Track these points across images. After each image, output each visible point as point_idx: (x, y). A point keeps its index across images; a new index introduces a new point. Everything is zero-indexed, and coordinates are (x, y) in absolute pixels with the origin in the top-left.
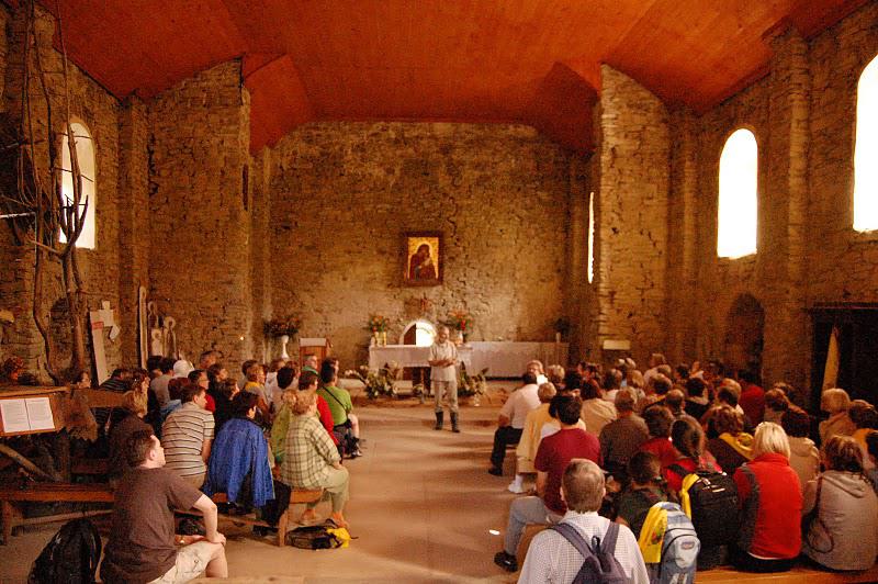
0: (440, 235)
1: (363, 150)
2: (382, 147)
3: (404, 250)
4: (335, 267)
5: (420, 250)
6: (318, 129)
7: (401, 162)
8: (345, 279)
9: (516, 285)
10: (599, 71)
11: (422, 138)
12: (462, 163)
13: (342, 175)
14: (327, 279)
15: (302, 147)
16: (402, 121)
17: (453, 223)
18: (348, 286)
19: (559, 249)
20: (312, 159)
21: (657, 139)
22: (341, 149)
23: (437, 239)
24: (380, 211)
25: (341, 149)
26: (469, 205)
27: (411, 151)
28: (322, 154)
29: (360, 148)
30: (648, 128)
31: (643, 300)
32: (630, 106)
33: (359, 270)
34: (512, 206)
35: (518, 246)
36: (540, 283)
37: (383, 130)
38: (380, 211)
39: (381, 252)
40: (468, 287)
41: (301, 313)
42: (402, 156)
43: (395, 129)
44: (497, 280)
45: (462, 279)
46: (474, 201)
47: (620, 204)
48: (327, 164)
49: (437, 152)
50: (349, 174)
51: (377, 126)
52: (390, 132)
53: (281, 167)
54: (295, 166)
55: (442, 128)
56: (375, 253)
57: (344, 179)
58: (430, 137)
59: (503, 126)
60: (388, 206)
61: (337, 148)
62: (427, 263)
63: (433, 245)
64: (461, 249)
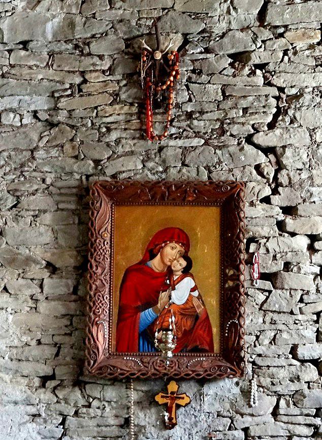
17: (267, 151)
64: (302, 242)
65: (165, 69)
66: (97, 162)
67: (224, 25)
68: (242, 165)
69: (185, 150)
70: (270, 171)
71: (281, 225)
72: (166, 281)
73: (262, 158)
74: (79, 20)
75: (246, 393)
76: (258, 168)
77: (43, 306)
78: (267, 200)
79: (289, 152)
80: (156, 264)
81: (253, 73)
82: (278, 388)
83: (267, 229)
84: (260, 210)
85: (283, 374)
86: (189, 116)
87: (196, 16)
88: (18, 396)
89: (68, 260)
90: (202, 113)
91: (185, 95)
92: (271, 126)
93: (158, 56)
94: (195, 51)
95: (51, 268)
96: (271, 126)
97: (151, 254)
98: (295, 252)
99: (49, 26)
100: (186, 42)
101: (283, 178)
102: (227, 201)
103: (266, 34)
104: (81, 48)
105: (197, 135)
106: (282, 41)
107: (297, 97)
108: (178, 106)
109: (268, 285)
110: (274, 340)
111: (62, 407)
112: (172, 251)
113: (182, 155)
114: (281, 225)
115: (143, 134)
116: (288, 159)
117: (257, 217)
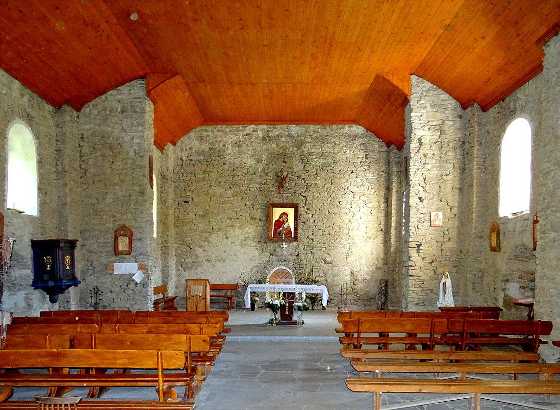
0: (296, 207)
2: (253, 144)
3: (269, 216)
4: (220, 230)
5: (280, 217)
6: (206, 131)
8: (227, 238)
9: (349, 241)
10: (409, 80)
11: (282, 137)
12: (310, 154)
13: (224, 164)
15: (196, 145)
16: (268, 125)
17: (304, 197)
19: (382, 216)
20: (202, 153)
21: (452, 131)
22: (224, 145)
23: (293, 209)
24: (252, 189)
25: (224, 145)
26: (315, 184)
27: (274, 145)
29: (238, 145)
30: (446, 122)
31: (442, 250)
32: (433, 107)
33: (238, 231)
34: (348, 185)
36: (368, 239)
39: (252, 218)
40: (315, 243)
41: (196, 262)
42: (267, 150)
43: (263, 130)
44: (336, 237)
46: (320, 181)
47: (425, 179)
48: (214, 156)
49: (293, 146)
51: (250, 128)
52: (259, 132)
53: (181, 159)
54: (190, 158)
55: (295, 129)
56: (249, 219)
57: (226, 167)
58: (286, 136)
60: (258, 186)
61: (221, 145)
63: (291, 212)
65: (285, 178)
66: (270, 199)
68: (299, 200)
69: (288, 196)
71: (306, 212)
72: (283, 222)
73: (303, 198)
75: (298, 245)
77: (259, 228)
78: (304, 207)
79: (308, 197)
80: (281, 220)
82: (305, 244)
85: (305, 241)
88: (254, 245)
89: (264, 218)
91: (288, 185)
92: (305, 191)
93: (282, 177)
94: (290, 175)
95: (260, 220)
96: (305, 191)
99: (260, 169)
100: (288, 173)
101: (307, 203)
107: (311, 185)
108: (286, 187)
109: (303, 224)
112: (284, 217)
114: (306, 212)
115: (279, 193)
116: (308, 198)
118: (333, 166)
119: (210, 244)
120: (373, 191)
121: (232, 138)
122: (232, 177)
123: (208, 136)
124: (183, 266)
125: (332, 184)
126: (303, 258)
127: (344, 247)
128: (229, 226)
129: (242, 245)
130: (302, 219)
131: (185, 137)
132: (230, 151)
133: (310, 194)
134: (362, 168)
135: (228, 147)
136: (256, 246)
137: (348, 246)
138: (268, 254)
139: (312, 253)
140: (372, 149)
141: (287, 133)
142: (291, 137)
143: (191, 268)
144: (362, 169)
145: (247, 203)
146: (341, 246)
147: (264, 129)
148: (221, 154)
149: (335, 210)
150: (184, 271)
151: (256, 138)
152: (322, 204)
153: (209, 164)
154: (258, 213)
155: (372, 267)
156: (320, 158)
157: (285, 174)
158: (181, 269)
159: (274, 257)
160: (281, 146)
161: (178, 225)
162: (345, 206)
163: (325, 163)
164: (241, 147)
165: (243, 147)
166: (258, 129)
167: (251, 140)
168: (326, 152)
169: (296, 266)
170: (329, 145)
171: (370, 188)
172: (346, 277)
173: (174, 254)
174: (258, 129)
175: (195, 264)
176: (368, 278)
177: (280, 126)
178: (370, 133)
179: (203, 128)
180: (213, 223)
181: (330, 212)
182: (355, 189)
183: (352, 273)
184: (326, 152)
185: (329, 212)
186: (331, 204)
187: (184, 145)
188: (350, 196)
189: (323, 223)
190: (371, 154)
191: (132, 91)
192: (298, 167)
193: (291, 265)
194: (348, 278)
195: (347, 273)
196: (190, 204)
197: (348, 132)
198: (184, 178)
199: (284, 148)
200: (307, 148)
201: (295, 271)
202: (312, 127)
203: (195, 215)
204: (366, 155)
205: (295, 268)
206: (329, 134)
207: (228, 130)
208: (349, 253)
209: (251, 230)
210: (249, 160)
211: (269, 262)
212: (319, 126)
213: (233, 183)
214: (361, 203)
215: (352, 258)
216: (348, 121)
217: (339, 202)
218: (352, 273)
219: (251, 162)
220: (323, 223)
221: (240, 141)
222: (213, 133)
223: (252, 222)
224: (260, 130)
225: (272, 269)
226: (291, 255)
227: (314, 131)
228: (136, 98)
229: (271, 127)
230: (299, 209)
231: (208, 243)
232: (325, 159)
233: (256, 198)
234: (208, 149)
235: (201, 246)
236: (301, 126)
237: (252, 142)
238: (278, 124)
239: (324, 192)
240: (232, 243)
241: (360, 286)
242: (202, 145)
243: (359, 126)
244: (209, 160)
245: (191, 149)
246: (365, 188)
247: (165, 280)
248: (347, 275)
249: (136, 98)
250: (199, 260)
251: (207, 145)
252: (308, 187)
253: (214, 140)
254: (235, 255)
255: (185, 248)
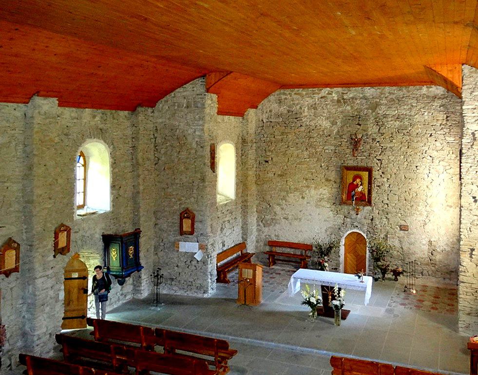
1: (315, 108)
2: (328, 107)
4: (296, 189)
6: (284, 94)
7: (341, 116)
8: (303, 198)
11: (356, 99)
12: (385, 116)
13: (301, 126)
14: (291, 198)
17: (379, 160)
18: (305, 203)
22: (301, 108)
23: (368, 173)
24: (327, 151)
25: (301, 108)
27: (349, 108)
28: (289, 111)
29: (314, 107)
33: (313, 192)
34: (426, 148)
35: (429, 179)
36: (448, 208)
37: (329, 94)
38: (327, 151)
39: (327, 180)
40: (390, 208)
41: (274, 219)
42: (342, 112)
44: (412, 204)
45: (386, 201)
46: (396, 144)
48: (293, 117)
49: (367, 109)
50: (307, 126)
51: (325, 91)
52: (334, 95)
53: (262, 120)
54: (270, 120)
55: (369, 91)
56: (323, 181)
57: (303, 129)
59: (418, 87)
60: (333, 148)
61: (298, 107)
62: (360, 189)
63: (365, 175)
64: (385, 180)
67: (371, 133)
68: (374, 164)
69: (362, 159)
70: (379, 165)
71: (381, 176)
72: (357, 186)
73: (378, 161)
74: (340, 131)
75: (373, 209)
76: (377, 163)
78: (378, 170)
80: (355, 183)
81: (376, 143)
83: (378, 177)
84: (377, 172)
86: (363, 152)
87: (365, 131)
88: (328, 206)
89: (338, 181)
90: (365, 151)
91: (362, 148)
92: (380, 155)
93: (356, 140)
95: (335, 182)
96: (380, 155)
97: (354, 180)
98: (383, 182)
100: (363, 136)
101: (382, 166)
102: (369, 170)
103: (380, 135)
104: (341, 137)
105: (364, 156)
106: (383, 137)
110: (378, 199)
111: (337, 209)
112: (358, 180)
113: (361, 160)
114: (381, 176)
117: (376, 174)
118: (410, 129)
119: (287, 203)
120: (454, 156)
121: (309, 101)
122: (308, 138)
123: (286, 99)
124: (263, 222)
125: (408, 147)
126: (378, 223)
127: (421, 214)
128: (304, 187)
129: (317, 206)
130: (377, 183)
131: (266, 100)
132: (306, 114)
133: (385, 158)
134: (442, 131)
135: (304, 110)
136: (330, 207)
137: (425, 214)
138: (342, 216)
139: (386, 218)
140: (453, 110)
141: (361, 96)
142: (366, 99)
143: (270, 225)
144: (442, 132)
145: (323, 165)
146: (418, 213)
147: (339, 92)
148: (298, 116)
149: (412, 175)
150: (264, 227)
151: (331, 101)
152: (397, 168)
153: (287, 126)
154: (333, 175)
155: (452, 238)
156: (395, 121)
157: (359, 136)
158: (261, 224)
159: (349, 220)
160: (356, 108)
161: (259, 183)
162: (423, 170)
163: (401, 126)
164: (317, 110)
165: (320, 111)
166: (332, 92)
167: (326, 102)
168: (402, 115)
169: (370, 230)
170: (405, 107)
171: (451, 152)
172: (422, 247)
173: (255, 210)
174: (332, 92)
175: (274, 221)
176: (448, 249)
177: (354, 89)
178: (451, 93)
179: (282, 91)
180: (290, 183)
181: (406, 177)
182: (434, 154)
183: (430, 242)
184: (402, 115)
185: (405, 177)
186: (408, 168)
187: (264, 107)
188: (428, 161)
189: (399, 188)
190: (452, 115)
191: (195, 89)
192: (372, 129)
193: (365, 229)
194: (426, 248)
195: (424, 242)
196: (270, 163)
197: (426, 93)
198: (264, 139)
199: (359, 110)
200: (381, 110)
201: (369, 235)
202: (387, 89)
203: (274, 174)
204: (447, 117)
205: (369, 232)
206: (405, 96)
207: (304, 93)
208: (427, 221)
209: (326, 191)
210: (324, 123)
211: (343, 224)
212: (394, 88)
213: (309, 145)
214: (441, 168)
215: (429, 227)
216: (425, 82)
217: (417, 167)
218: (430, 242)
219: (326, 124)
220: (399, 188)
221: (315, 104)
222: (291, 96)
223: (327, 183)
224: (335, 93)
225: (346, 231)
226: (365, 218)
227: (389, 93)
228: (198, 95)
229: (346, 89)
230: (374, 172)
231: (286, 201)
232: (401, 122)
233: (331, 159)
234: (286, 112)
235: (279, 205)
236: (376, 88)
237: (327, 104)
238: (352, 87)
239: (400, 156)
240: (307, 203)
241: (438, 257)
242: (280, 108)
243: (438, 87)
244: (287, 123)
245: (271, 111)
246: (446, 152)
247: (245, 236)
248: (424, 245)
249: (198, 95)
250: (277, 217)
251: (285, 107)
252: (383, 150)
253: (292, 103)
254: (310, 215)
255: (265, 205)
